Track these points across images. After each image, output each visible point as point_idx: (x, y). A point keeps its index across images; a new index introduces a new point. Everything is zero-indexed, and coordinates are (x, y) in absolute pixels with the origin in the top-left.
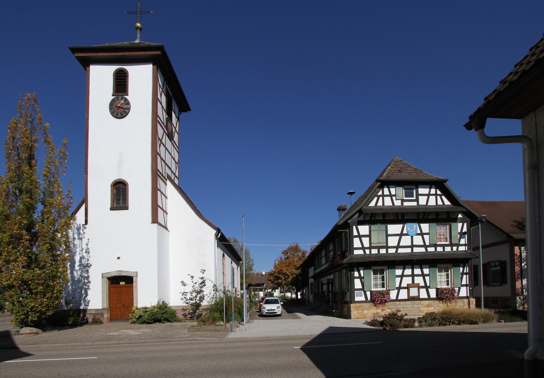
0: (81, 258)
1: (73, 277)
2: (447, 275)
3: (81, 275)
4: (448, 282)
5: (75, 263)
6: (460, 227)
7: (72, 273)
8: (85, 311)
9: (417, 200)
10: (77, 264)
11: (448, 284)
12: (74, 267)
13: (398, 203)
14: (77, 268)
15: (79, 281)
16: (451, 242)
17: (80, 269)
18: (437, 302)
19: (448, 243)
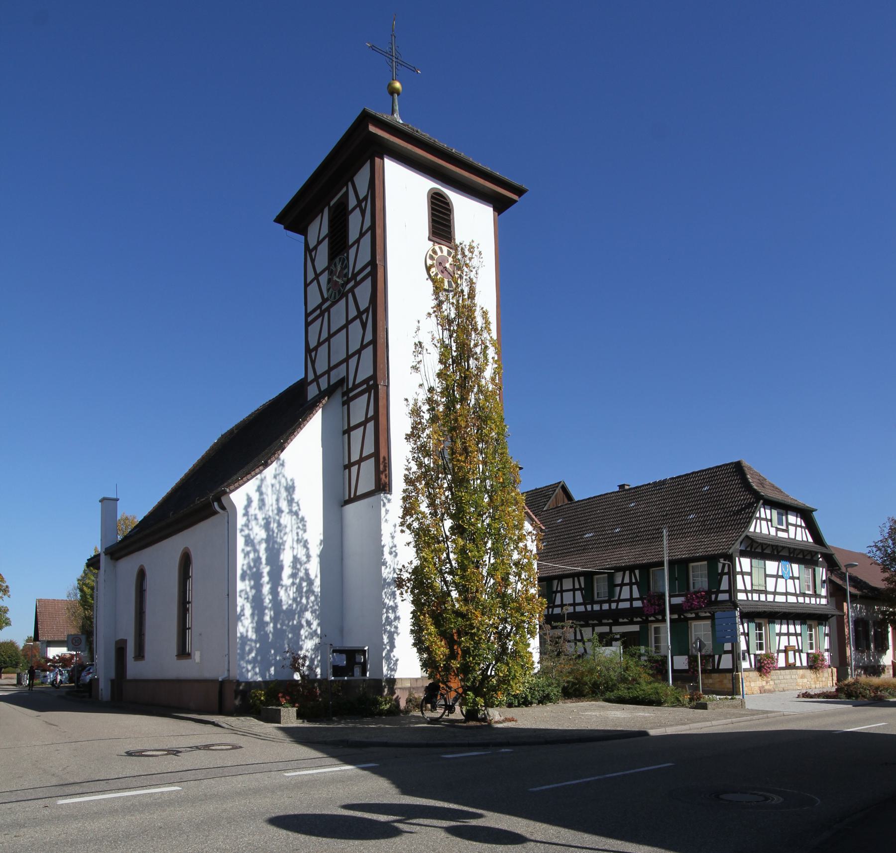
0: (296, 560)
1: (276, 602)
2: (811, 635)
3: (294, 599)
4: (811, 644)
5: (281, 568)
6: (822, 573)
7: (274, 592)
8: (392, 682)
9: (787, 531)
10: (287, 572)
11: (811, 648)
12: (280, 579)
13: (773, 532)
14: (286, 580)
15: (290, 613)
16: (815, 592)
17: (293, 584)
18: (809, 671)
19: (810, 592)
